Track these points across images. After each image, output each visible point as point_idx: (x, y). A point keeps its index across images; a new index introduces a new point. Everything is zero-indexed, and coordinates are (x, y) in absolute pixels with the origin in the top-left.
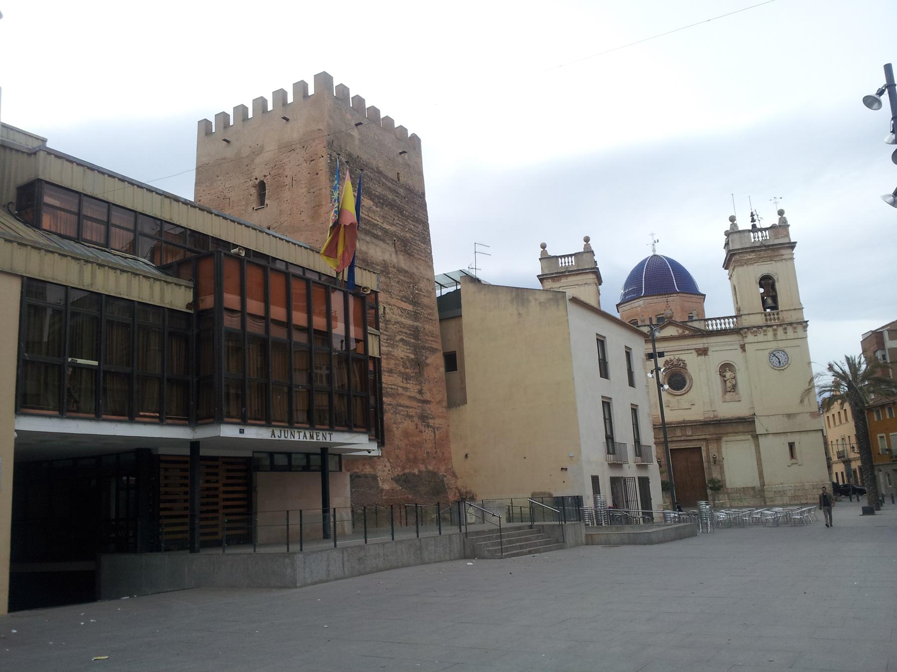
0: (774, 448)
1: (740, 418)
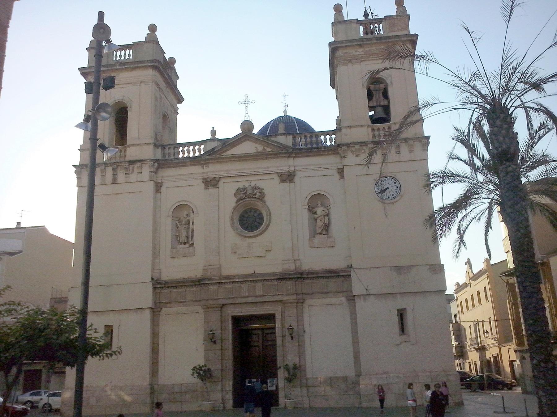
0: (377, 316)
1: (330, 271)
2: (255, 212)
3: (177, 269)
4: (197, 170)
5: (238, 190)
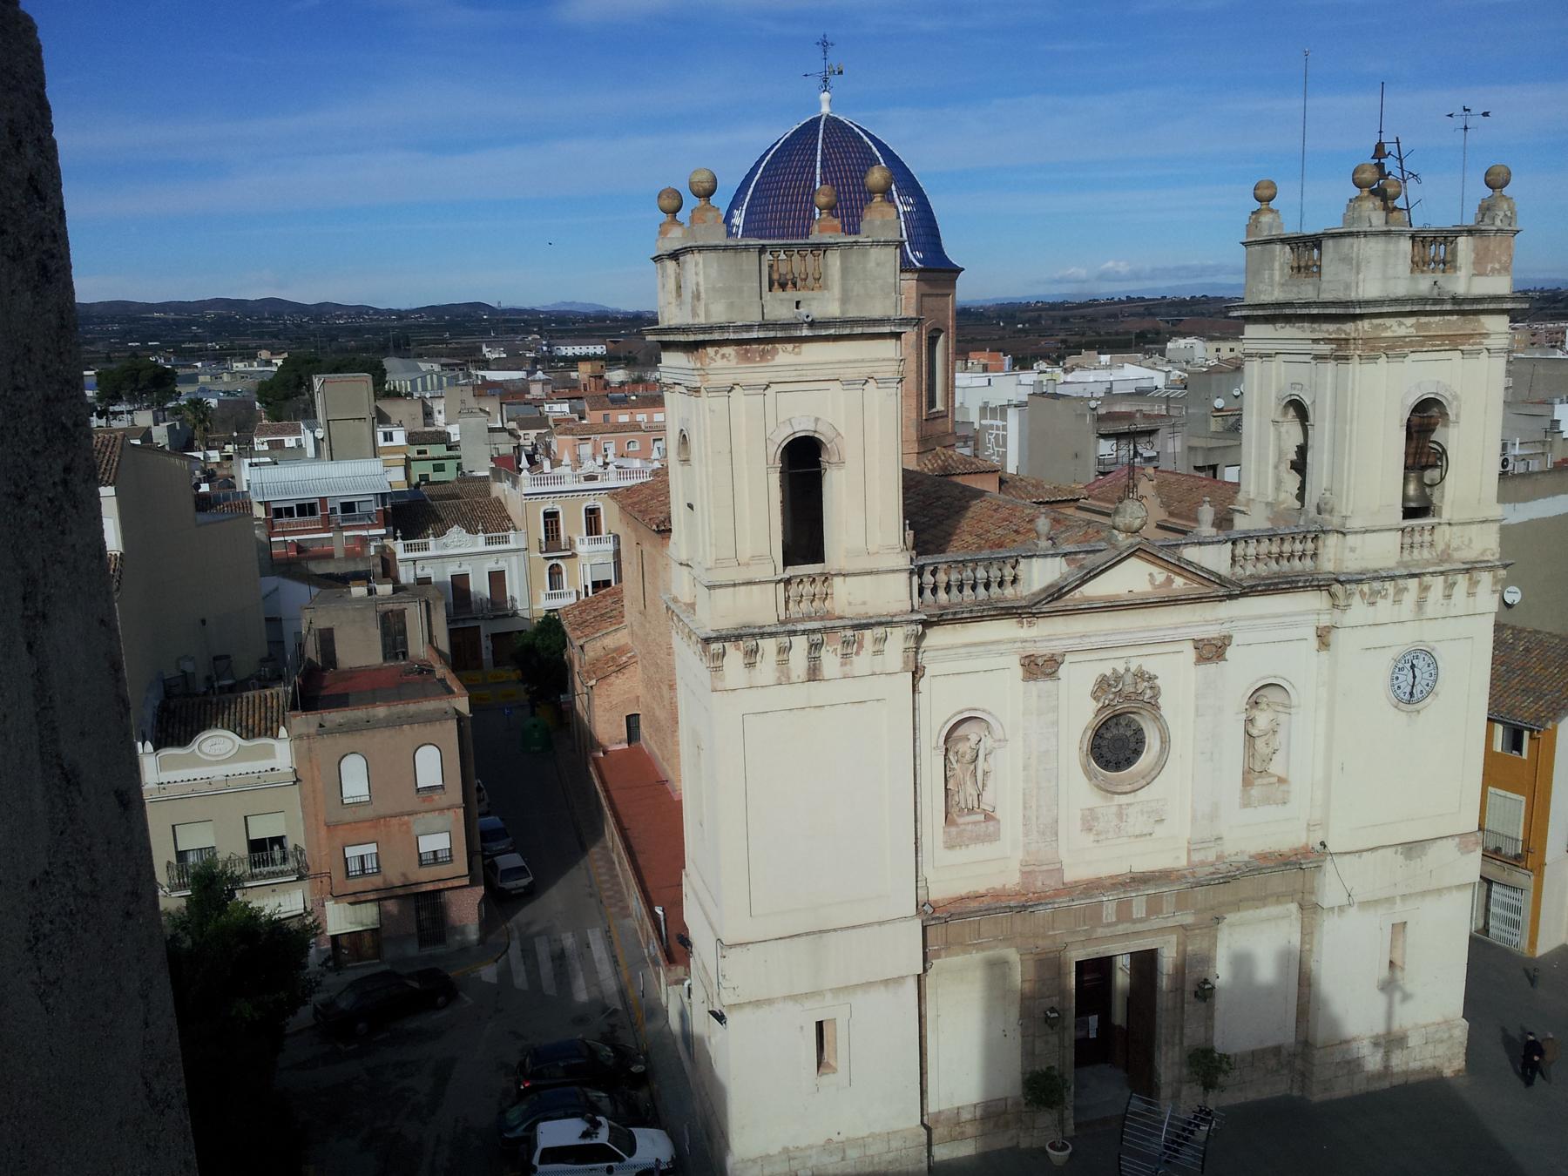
3: (962, 872)
4: (1006, 629)
5: (1103, 684)
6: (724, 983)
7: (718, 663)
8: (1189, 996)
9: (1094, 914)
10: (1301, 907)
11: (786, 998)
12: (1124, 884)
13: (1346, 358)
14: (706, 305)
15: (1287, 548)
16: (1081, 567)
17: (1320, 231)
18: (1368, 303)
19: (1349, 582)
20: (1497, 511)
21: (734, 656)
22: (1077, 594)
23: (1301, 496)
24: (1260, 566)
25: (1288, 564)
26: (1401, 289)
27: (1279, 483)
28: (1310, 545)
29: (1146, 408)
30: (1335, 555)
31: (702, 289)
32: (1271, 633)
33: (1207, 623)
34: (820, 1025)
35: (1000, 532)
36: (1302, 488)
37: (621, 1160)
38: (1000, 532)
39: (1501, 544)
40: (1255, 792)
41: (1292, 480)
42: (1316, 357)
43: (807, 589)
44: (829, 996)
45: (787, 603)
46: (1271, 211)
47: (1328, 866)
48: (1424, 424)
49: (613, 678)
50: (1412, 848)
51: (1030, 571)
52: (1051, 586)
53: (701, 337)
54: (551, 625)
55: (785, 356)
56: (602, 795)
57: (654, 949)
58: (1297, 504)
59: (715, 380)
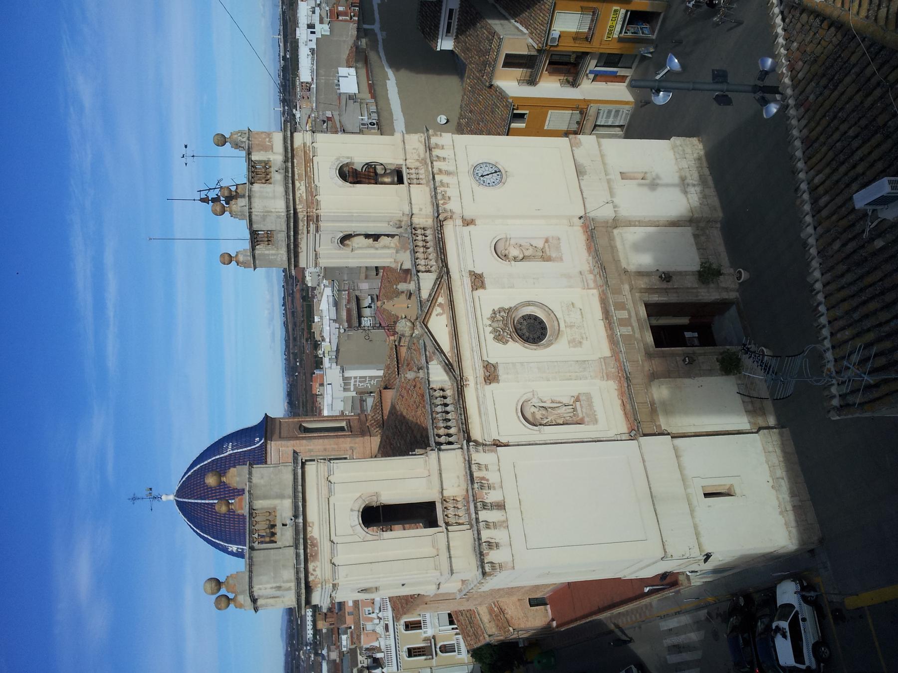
2: (521, 324)
3: (609, 413)
4: (470, 394)
5: (499, 338)
6: (687, 555)
7: (497, 566)
8: (669, 285)
9: (627, 338)
10: (616, 227)
11: (693, 517)
12: (610, 324)
13: (317, 216)
14: (284, 582)
15: (420, 244)
16: (434, 353)
17: (248, 231)
18: (287, 207)
19: (438, 211)
20: (398, 136)
21: (493, 556)
22: (449, 355)
23: (392, 236)
24: (431, 257)
25: (429, 241)
26: (279, 189)
27: (385, 247)
28: (419, 232)
29: (344, 302)
30: (424, 218)
31: (274, 585)
32: (466, 251)
33: (463, 284)
34: (707, 495)
35: (415, 395)
36: (388, 236)
37: (797, 613)
38: (415, 395)
39: (416, 133)
40: (554, 255)
41: (384, 241)
42: (317, 231)
43: (451, 512)
44: (689, 491)
45: (460, 524)
46: (237, 255)
47: (592, 215)
48: (352, 175)
49: (508, 616)
50: (580, 172)
51: (437, 382)
52: (445, 370)
53: (303, 585)
54: (477, 653)
55: (314, 532)
56: (578, 623)
57: (670, 593)
58: (397, 237)
59: (328, 574)
